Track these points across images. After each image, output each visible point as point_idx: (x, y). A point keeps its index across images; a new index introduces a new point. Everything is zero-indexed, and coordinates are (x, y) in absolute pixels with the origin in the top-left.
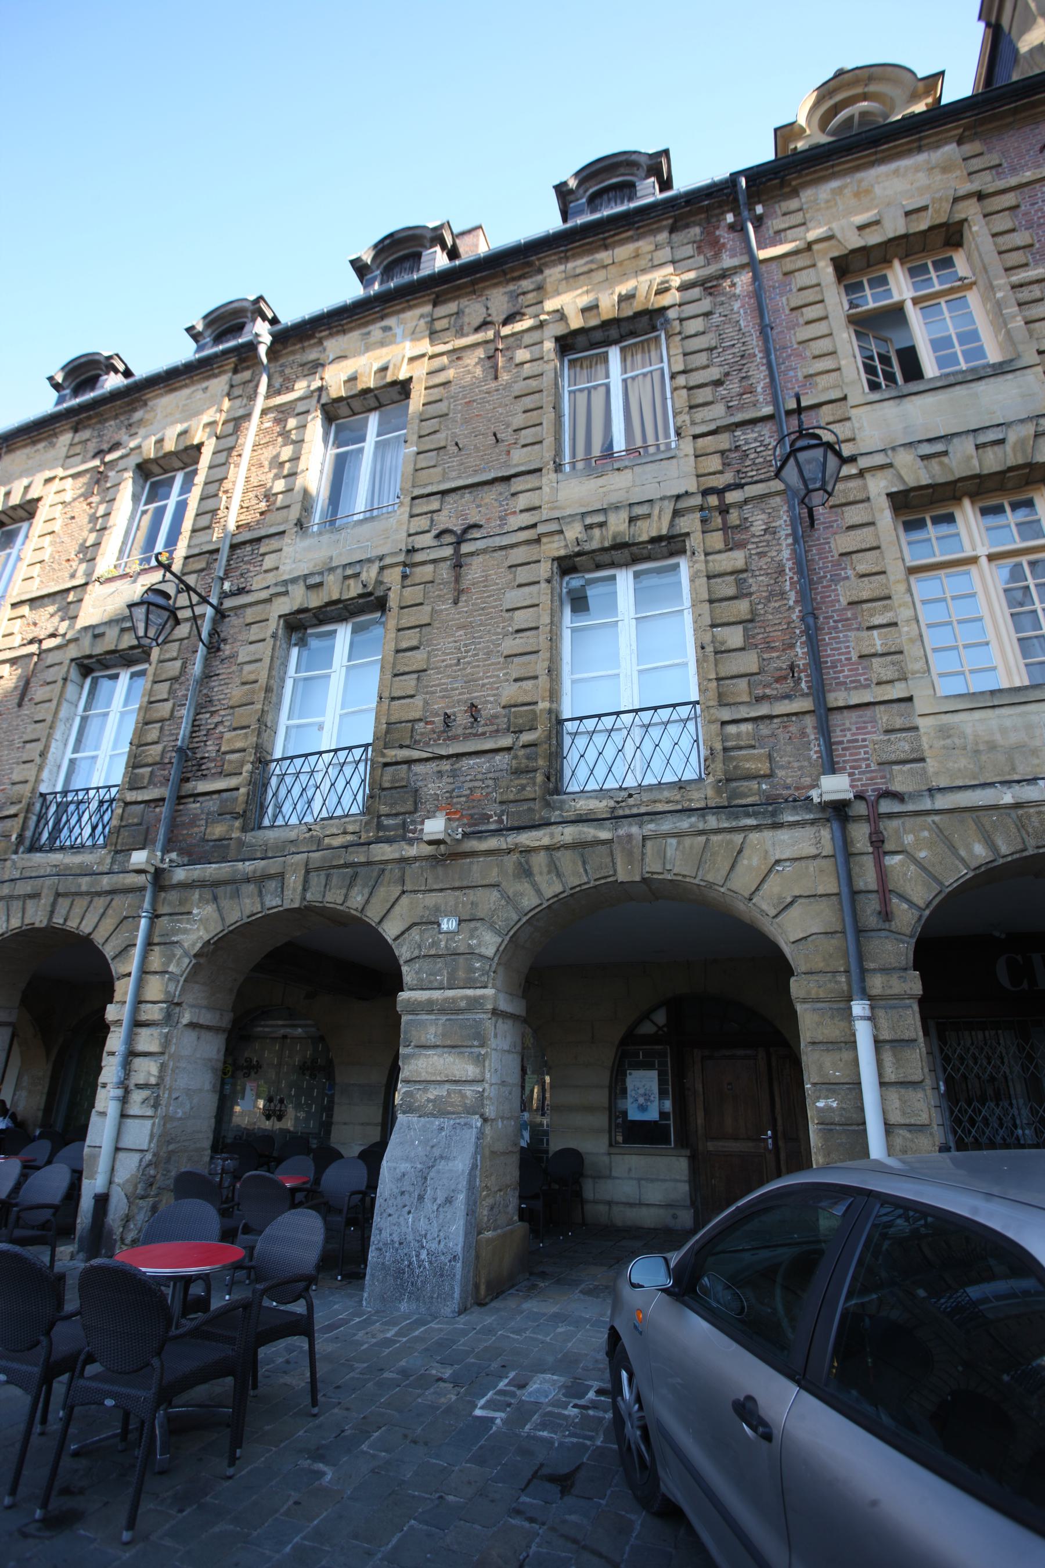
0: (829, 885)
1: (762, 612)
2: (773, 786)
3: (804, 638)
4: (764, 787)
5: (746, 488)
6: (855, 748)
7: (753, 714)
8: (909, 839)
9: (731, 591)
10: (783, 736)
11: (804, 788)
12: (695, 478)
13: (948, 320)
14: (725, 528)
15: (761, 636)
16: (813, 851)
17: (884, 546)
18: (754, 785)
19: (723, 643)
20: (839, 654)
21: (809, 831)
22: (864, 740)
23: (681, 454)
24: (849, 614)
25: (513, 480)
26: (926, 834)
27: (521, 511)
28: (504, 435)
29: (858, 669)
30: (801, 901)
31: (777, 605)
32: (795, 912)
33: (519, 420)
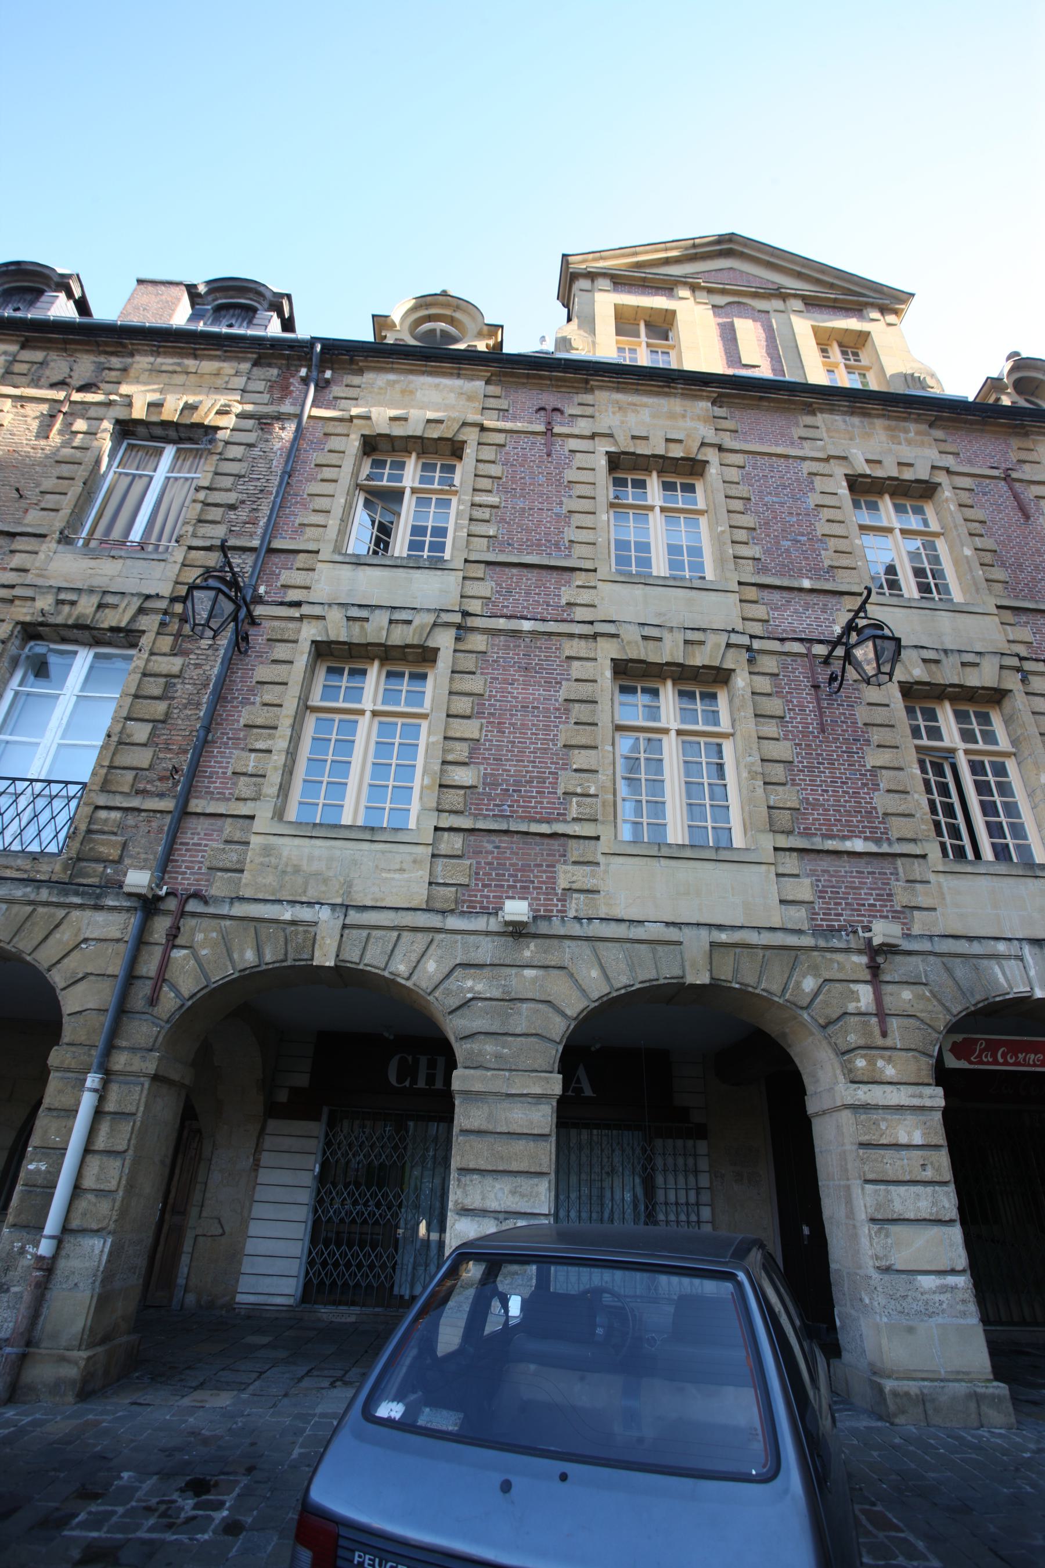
0: (116, 967)
7: (125, 805)
9: (157, 691)
10: (144, 828)
13: (432, 514)
16: (118, 935)
18: (100, 867)
19: (129, 736)
20: (220, 767)
21: (119, 918)
22: (206, 846)
23: (171, 559)
25: (18, 538)
26: (214, 935)
27: (12, 569)
28: (30, 493)
31: (189, 713)
33: (48, 484)
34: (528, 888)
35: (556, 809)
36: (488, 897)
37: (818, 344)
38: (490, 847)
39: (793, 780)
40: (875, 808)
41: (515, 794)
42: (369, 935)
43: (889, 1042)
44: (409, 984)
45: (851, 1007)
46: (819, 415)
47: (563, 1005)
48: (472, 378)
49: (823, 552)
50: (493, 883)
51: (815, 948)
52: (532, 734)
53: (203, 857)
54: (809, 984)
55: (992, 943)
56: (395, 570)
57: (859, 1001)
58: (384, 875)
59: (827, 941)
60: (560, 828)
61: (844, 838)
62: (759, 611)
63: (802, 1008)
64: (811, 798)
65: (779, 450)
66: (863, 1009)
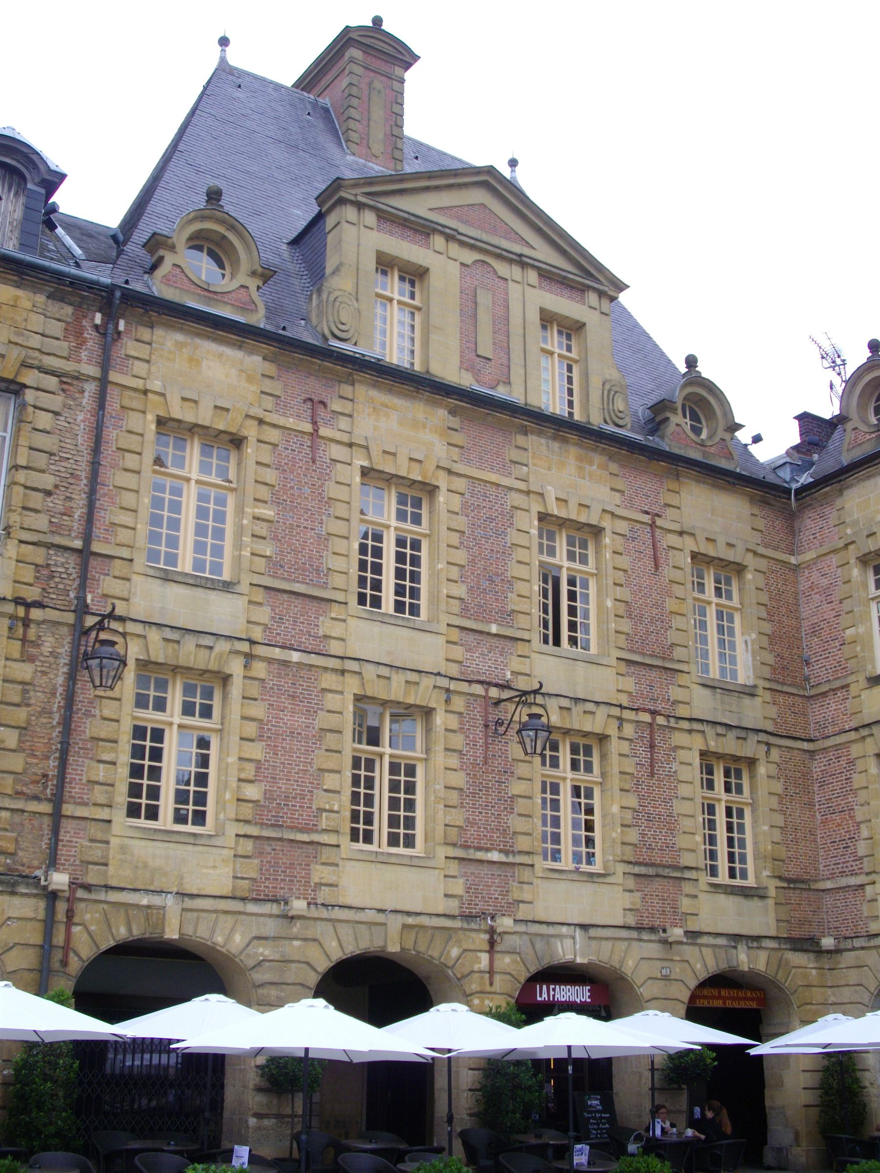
0: (37, 938)
1: (34, 723)
2: (14, 862)
3: (57, 755)
4: (8, 861)
5: (47, 610)
6: (71, 846)
7: (13, 806)
8: (88, 916)
9: (16, 699)
10: (28, 826)
11: (33, 867)
12: (12, 584)
14: (24, 640)
15: (28, 743)
17: (124, 700)
20: (77, 774)
21: (32, 902)
22: (76, 842)
23: (7, 555)
24: (89, 745)
26: (97, 915)
29: (84, 789)
30: (18, 947)
31: (45, 721)
32: (13, 953)
34: (293, 881)
35: (311, 820)
36: (268, 887)
37: (541, 319)
38: (269, 849)
39: (462, 803)
40: (508, 827)
41: (285, 808)
42: (198, 918)
43: (493, 989)
44: (224, 950)
45: (476, 967)
46: (529, 435)
47: (315, 964)
48: (251, 353)
49: (509, 594)
50: (272, 877)
51: (462, 929)
52: (297, 757)
53: (75, 851)
54: (455, 952)
55: (559, 926)
56: (195, 589)
57: (480, 963)
58: (204, 871)
59: (468, 924)
60: (315, 837)
61: (488, 850)
62: (458, 652)
63: (448, 967)
64: (471, 818)
65: (494, 477)
66: (482, 969)
